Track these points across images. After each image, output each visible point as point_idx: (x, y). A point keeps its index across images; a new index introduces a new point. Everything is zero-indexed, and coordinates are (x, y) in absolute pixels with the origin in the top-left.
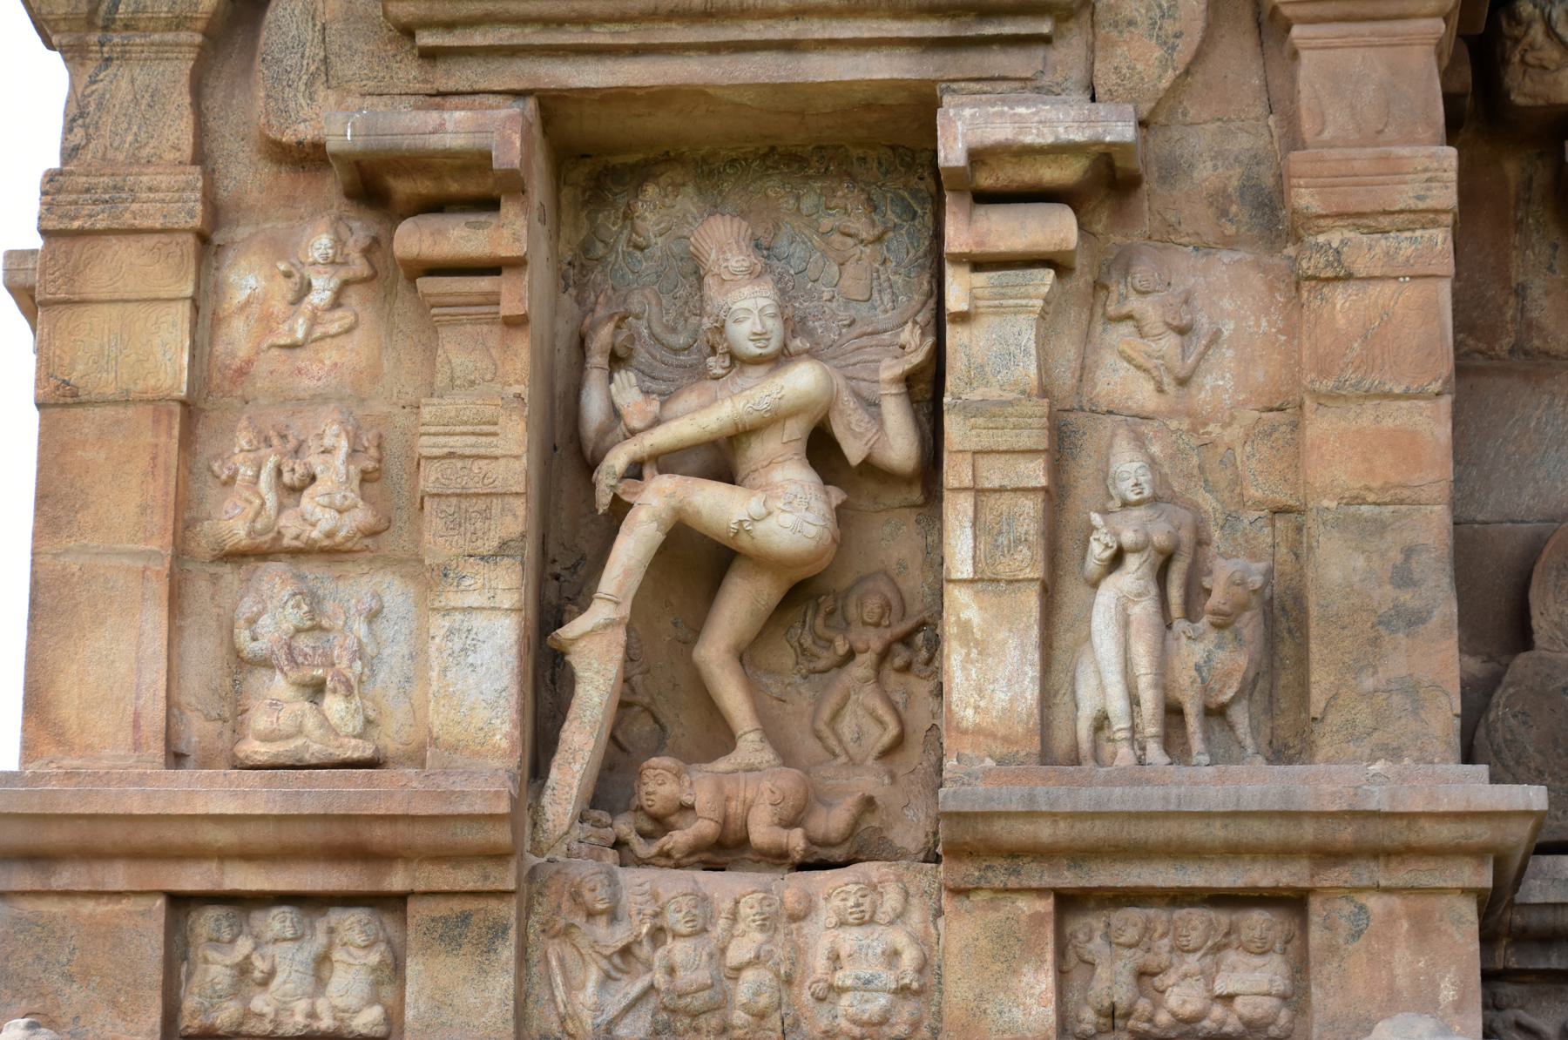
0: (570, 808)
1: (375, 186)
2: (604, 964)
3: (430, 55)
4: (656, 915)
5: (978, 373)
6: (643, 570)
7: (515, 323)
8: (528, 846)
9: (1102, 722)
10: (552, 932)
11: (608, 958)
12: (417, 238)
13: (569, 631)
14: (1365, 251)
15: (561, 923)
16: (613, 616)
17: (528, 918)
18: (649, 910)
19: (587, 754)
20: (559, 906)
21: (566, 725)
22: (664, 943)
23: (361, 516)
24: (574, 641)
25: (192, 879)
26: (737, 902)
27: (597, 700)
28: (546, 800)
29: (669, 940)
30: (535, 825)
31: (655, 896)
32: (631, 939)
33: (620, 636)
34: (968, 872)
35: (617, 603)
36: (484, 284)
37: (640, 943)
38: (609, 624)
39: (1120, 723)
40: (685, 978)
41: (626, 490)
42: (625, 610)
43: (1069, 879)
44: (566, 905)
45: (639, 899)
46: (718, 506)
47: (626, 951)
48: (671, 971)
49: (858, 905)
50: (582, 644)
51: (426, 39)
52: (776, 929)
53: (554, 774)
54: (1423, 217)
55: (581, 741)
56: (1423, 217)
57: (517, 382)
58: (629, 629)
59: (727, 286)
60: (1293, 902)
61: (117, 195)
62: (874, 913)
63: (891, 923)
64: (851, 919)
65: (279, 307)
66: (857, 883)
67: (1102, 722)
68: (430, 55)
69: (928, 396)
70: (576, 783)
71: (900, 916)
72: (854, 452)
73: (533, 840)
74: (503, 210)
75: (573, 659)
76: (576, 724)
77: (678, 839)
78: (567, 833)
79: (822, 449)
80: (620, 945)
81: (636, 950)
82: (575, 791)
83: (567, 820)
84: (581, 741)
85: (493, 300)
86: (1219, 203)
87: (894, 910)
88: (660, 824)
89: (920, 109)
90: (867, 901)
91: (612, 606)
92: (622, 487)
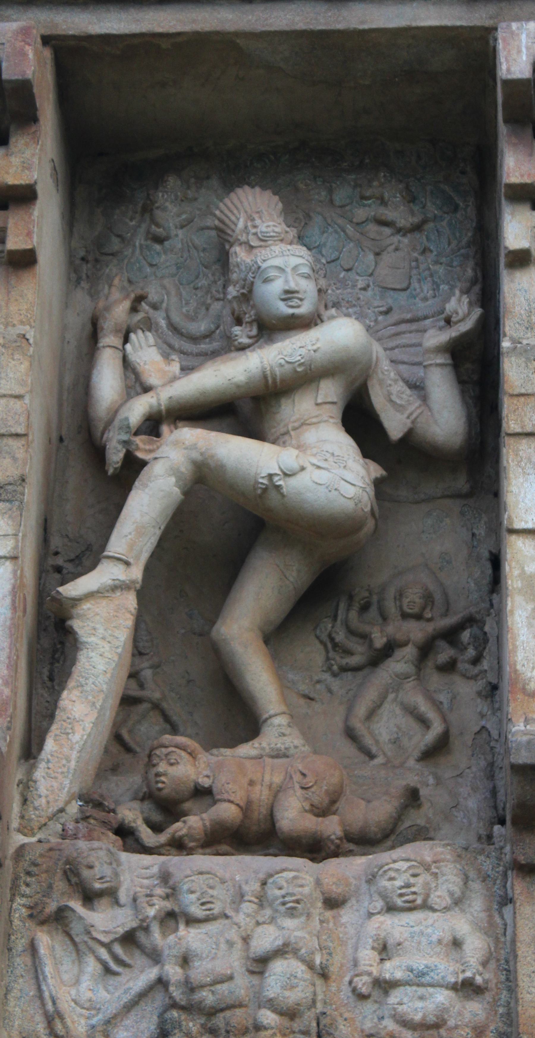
0: (67, 782)
2: (104, 954)
4: (167, 897)
6: (158, 533)
7: (25, 260)
8: (15, 824)
10: (42, 917)
11: (108, 946)
13: (72, 589)
15: (52, 907)
16: (122, 577)
17: (12, 900)
18: (160, 891)
19: (88, 726)
20: (50, 887)
21: (65, 694)
22: (176, 930)
24: (77, 601)
26: (264, 884)
27: (101, 667)
28: (39, 774)
29: (182, 927)
30: (25, 801)
31: (165, 877)
32: (134, 924)
33: (130, 601)
35: (127, 564)
37: (146, 929)
38: (119, 587)
40: (200, 971)
41: (142, 446)
42: (136, 573)
44: (60, 885)
45: (146, 882)
47: (129, 939)
48: (185, 961)
49: (408, 886)
50: (86, 606)
52: (309, 915)
53: (50, 745)
57: (22, 323)
58: (141, 595)
59: (256, 251)
62: (428, 896)
63: (447, 909)
64: (399, 902)
66: (408, 860)
69: (475, 377)
70: (74, 755)
71: (458, 902)
73: (22, 817)
74: (12, 140)
75: (76, 624)
76: (76, 693)
78: (62, 810)
80: (121, 931)
81: (141, 937)
82: (73, 764)
83: (63, 796)
87: (451, 894)
88: (167, 808)
90: (420, 880)
91: (122, 567)
92: (139, 440)
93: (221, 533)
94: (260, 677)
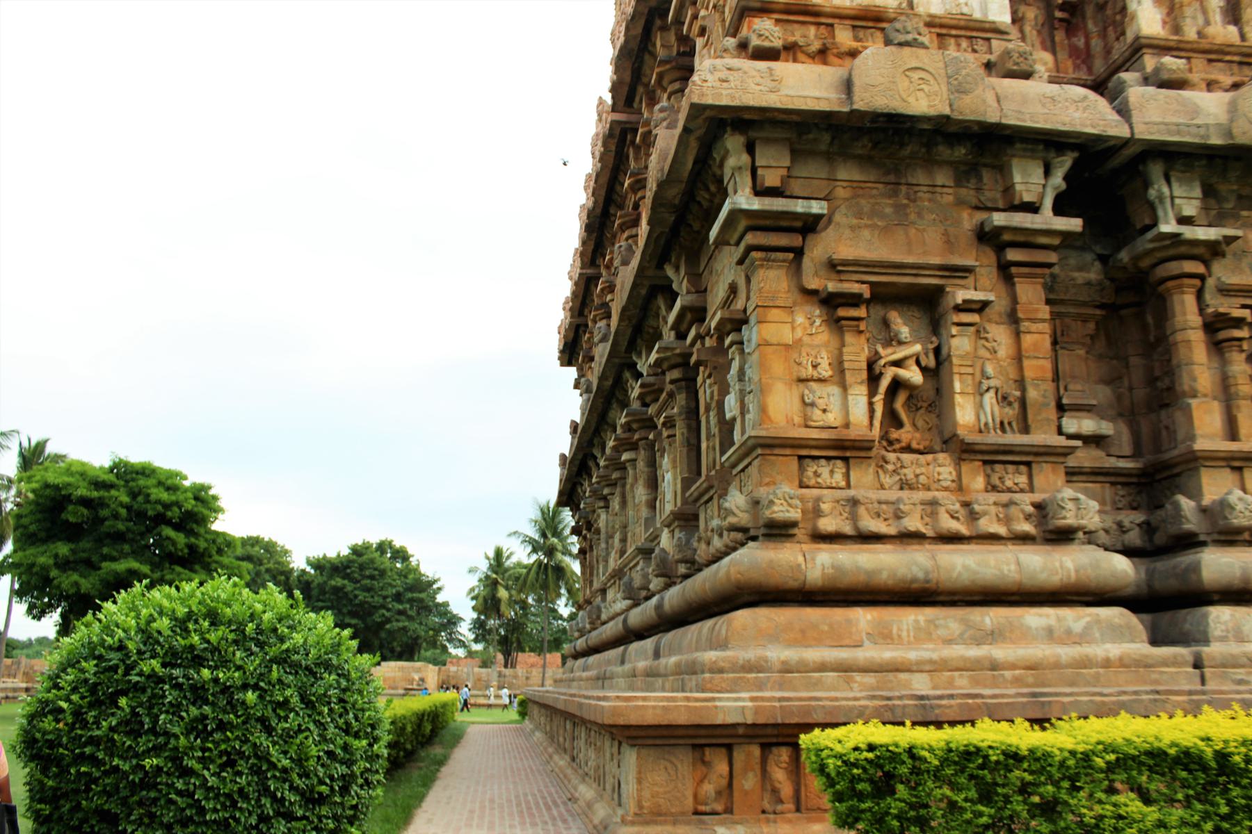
1: (830, 302)
3: (839, 272)
5: (957, 349)
9: (986, 424)
12: (842, 312)
14: (1034, 327)
23: (830, 373)
25: (804, 452)
34: (965, 456)
36: (855, 323)
39: (991, 425)
43: (987, 458)
46: (902, 373)
51: (840, 268)
54: (1043, 321)
55: (877, 423)
56: (1043, 321)
60: (1028, 464)
61: (773, 298)
65: (807, 325)
67: (986, 424)
68: (839, 272)
72: (923, 364)
77: (897, 446)
79: (918, 363)
84: (877, 423)
85: (858, 326)
86: (1000, 314)
89: (939, 291)
93: (897, 385)
94: (903, 416)
